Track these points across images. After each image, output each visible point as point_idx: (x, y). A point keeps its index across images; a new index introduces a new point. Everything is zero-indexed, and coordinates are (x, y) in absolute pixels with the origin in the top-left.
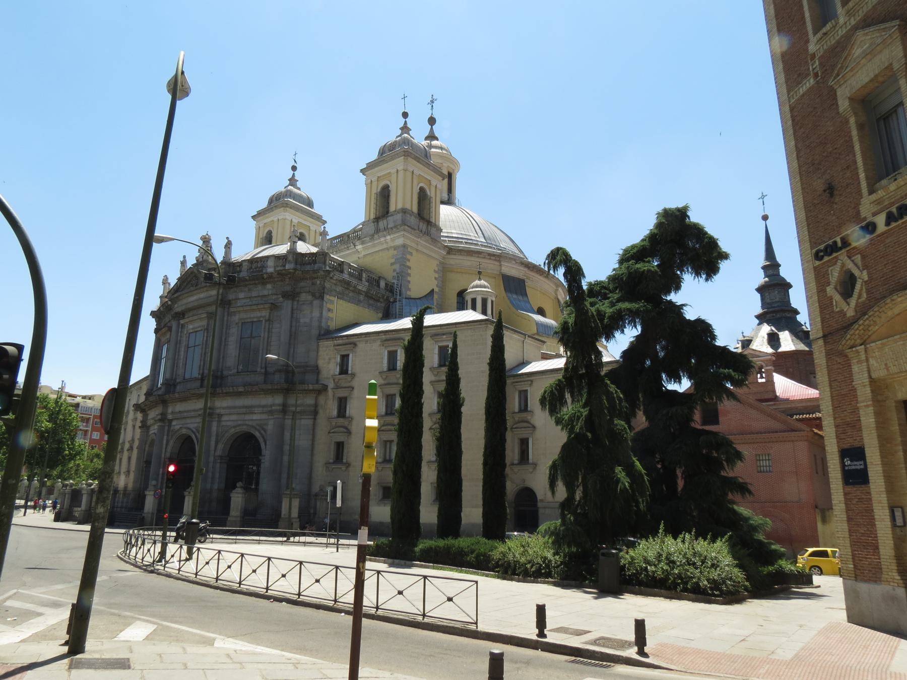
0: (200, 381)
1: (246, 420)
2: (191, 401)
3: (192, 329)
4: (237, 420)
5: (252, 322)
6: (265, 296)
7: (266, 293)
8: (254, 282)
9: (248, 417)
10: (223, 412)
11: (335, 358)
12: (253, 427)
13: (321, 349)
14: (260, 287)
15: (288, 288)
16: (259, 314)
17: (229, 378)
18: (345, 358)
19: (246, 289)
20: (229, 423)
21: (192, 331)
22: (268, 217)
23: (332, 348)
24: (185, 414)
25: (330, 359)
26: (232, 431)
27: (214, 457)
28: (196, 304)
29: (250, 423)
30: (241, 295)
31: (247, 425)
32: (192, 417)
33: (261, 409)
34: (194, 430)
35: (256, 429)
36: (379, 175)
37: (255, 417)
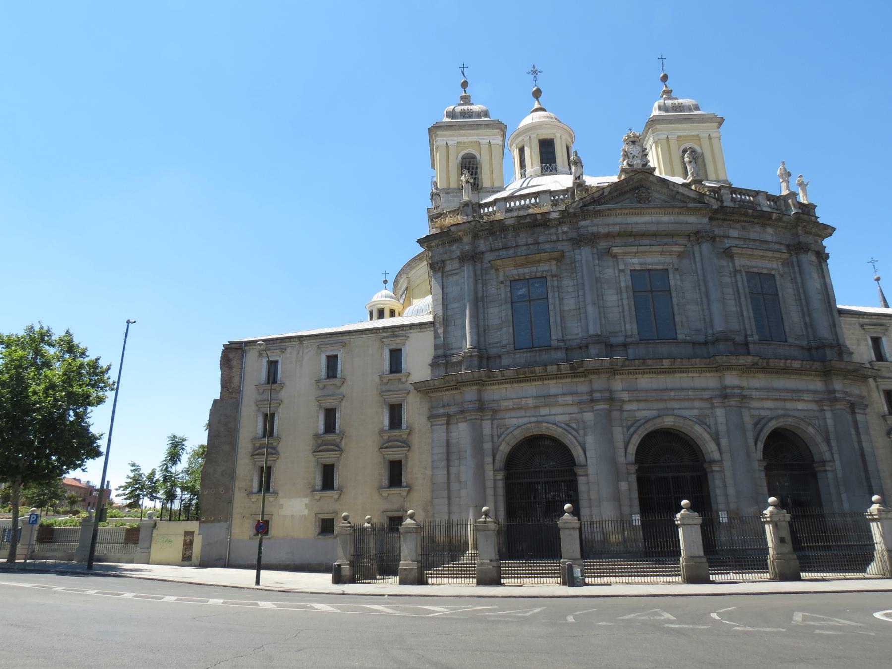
0: (691, 346)
1: (789, 410)
2: (685, 375)
3: (641, 264)
4: (775, 409)
5: (759, 274)
6: (766, 242)
7: (769, 238)
8: (752, 219)
9: (789, 405)
10: (755, 394)
11: (866, 340)
12: (802, 419)
13: (843, 326)
14: (758, 228)
15: (803, 239)
16: (769, 265)
17: (751, 346)
18: (876, 342)
19: (738, 226)
20: (763, 413)
21: (638, 267)
22: (464, 135)
23: (857, 326)
24: (672, 394)
25: (858, 340)
26: (773, 425)
27: (759, 461)
28: (653, 228)
29: (796, 414)
30: (734, 233)
31: (797, 418)
32: (689, 400)
33: (811, 395)
34: (695, 420)
35: (810, 424)
36: (679, 134)
37: (800, 406)
